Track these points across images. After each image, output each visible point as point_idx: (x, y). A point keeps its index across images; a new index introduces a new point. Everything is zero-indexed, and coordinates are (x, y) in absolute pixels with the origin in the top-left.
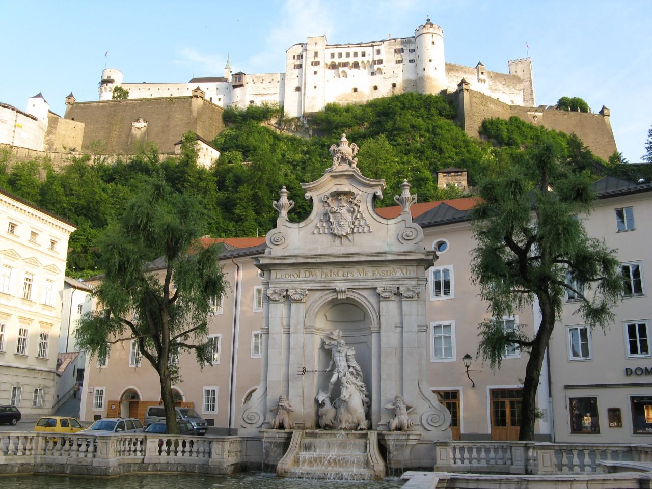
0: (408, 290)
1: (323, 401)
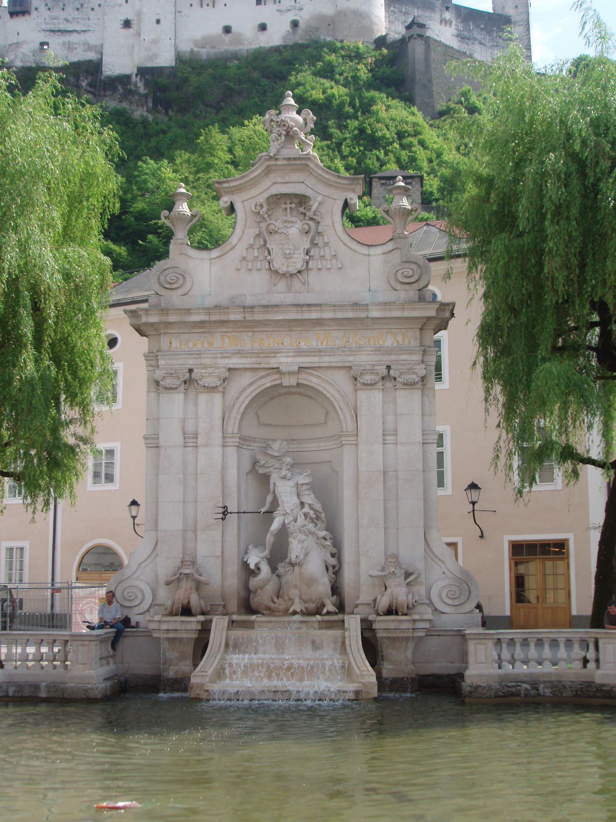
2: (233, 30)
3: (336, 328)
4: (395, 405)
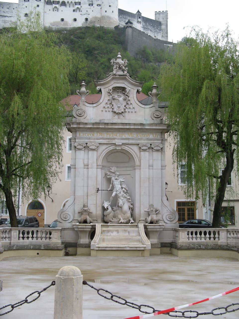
1: (107, 207)
2: (65, 20)
3: (134, 131)
4: (153, 157)
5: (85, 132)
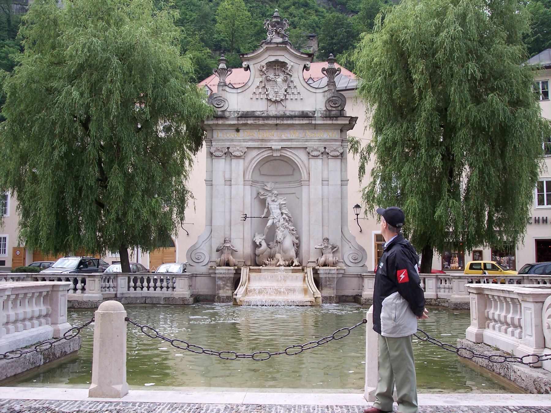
0: (335, 150)
4: (328, 166)
5: (226, 131)
